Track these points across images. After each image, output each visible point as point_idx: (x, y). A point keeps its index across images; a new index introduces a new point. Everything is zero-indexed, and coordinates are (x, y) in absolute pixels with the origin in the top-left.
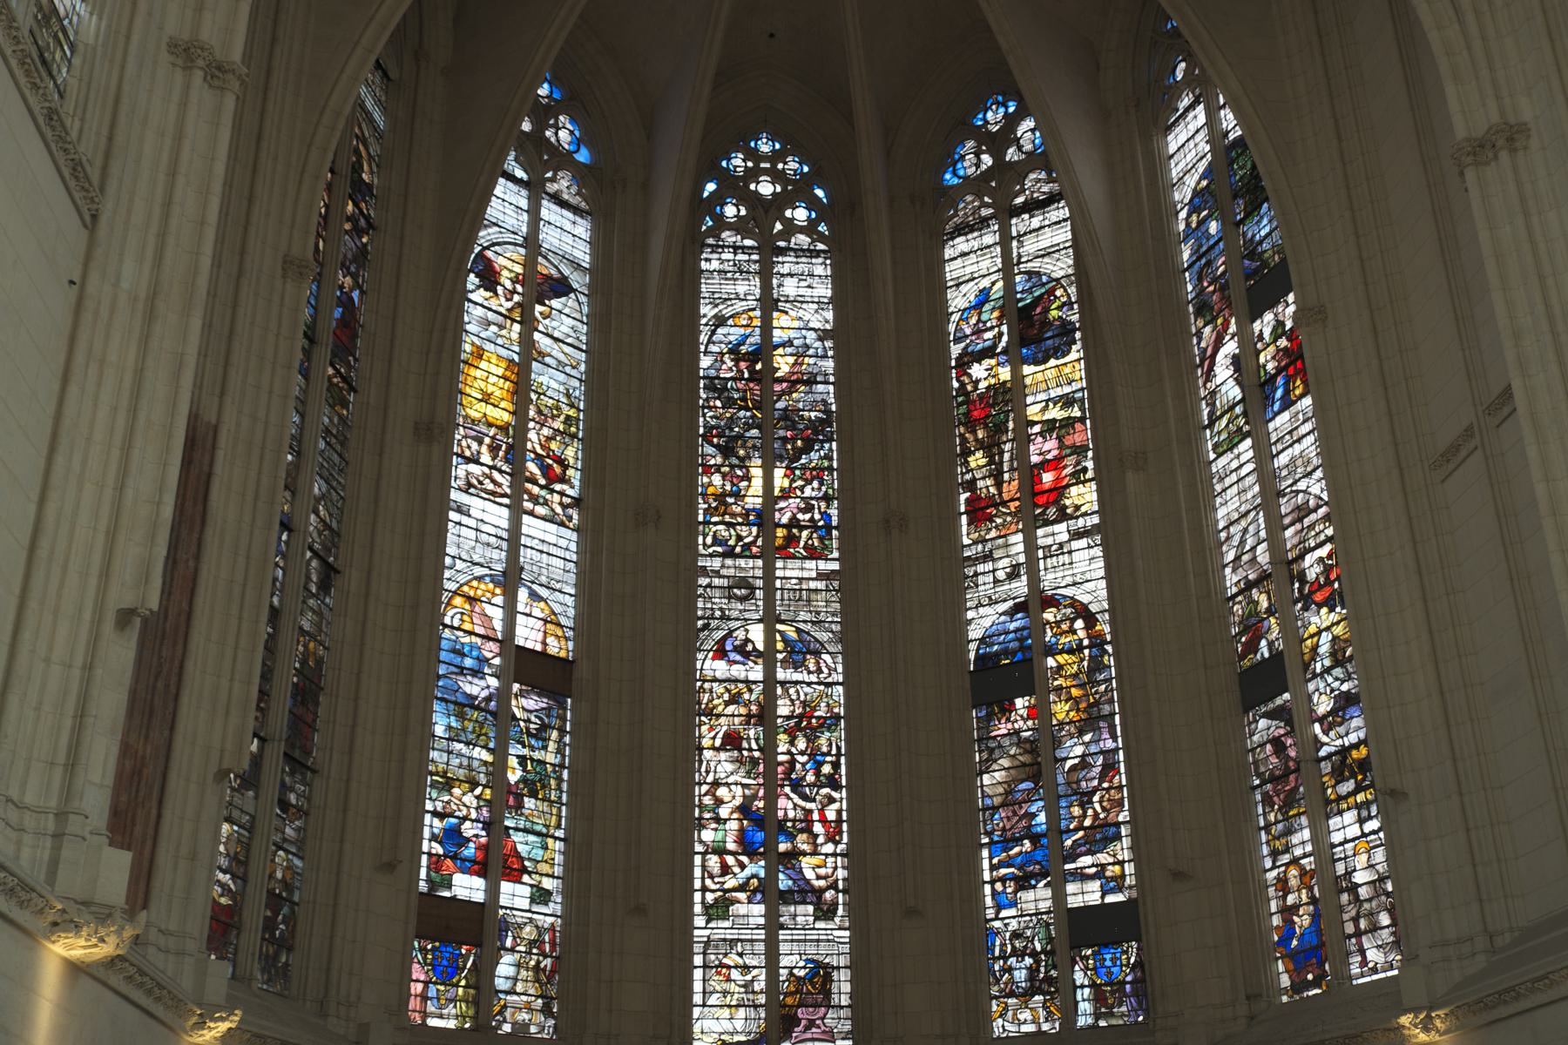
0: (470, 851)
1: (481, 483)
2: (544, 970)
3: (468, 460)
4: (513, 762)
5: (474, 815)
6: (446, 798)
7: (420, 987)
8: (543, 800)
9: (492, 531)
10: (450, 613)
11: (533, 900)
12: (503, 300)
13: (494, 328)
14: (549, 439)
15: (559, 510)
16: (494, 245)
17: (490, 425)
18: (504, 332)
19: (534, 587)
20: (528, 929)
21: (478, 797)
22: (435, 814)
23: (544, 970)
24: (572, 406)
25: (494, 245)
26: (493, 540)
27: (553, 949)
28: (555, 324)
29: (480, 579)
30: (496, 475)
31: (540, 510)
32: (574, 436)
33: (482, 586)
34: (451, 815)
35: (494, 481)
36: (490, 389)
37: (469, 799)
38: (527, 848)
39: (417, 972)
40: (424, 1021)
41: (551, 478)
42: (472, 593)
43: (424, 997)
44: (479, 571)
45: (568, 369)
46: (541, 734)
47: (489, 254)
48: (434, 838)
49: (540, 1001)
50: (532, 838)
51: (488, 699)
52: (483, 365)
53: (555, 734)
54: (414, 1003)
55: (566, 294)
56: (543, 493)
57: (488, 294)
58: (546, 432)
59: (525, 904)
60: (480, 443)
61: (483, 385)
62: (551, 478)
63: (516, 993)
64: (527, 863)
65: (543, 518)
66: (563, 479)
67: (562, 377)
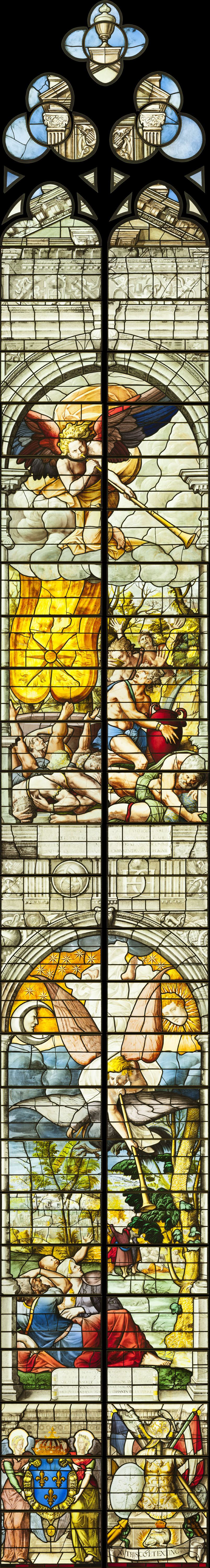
0: (74, 1336)
1: (52, 800)
2: (186, 1476)
3: (30, 773)
4: (117, 1201)
5: (76, 1289)
6: (32, 1274)
7: (18, 1518)
8: (170, 1245)
9: (74, 868)
10: (18, 1013)
11: (161, 1387)
12: (67, 480)
13: (55, 538)
14: (148, 687)
15: (172, 800)
16: (44, 391)
17: (60, 701)
18: (71, 538)
19: (137, 934)
20: (157, 1424)
21: (79, 1263)
22: (18, 1296)
23: (186, 1476)
24: (188, 614)
25: (44, 391)
26: (77, 883)
27: (198, 1446)
28: (148, 483)
29: (59, 949)
30: (76, 779)
31: (140, 810)
32: (191, 667)
33: (64, 958)
34: (42, 1294)
35: (74, 791)
36: (57, 641)
37: (67, 1266)
38: (151, 1317)
39: (11, 1501)
40: (27, 1559)
41: (155, 748)
42: (49, 975)
43: (26, 1531)
44: (57, 938)
45: (177, 554)
46: (162, 1152)
47: (40, 411)
48: (20, 1328)
49: (180, 1517)
50: (156, 1302)
51: (86, 1123)
52: (43, 607)
53: (185, 1147)
54: (9, 1539)
55: (165, 420)
56: (143, 781)
57: (41, 483)
58: (142, 677)
59: (151, 1393)
60: (46, 737)
61: (42, 639)
62: (155, 748)
63: (142, 1510)
64: (150, 1338)
65: (147, 822)
66: (177, 746)
67: (166, 573)
